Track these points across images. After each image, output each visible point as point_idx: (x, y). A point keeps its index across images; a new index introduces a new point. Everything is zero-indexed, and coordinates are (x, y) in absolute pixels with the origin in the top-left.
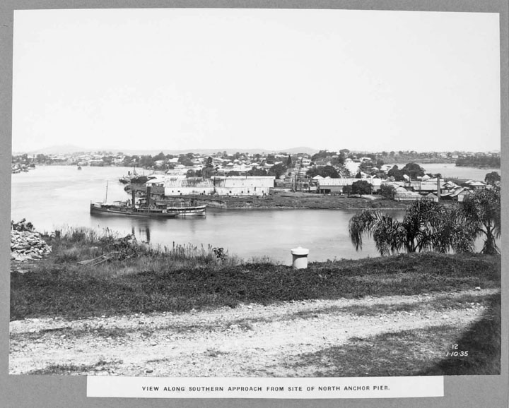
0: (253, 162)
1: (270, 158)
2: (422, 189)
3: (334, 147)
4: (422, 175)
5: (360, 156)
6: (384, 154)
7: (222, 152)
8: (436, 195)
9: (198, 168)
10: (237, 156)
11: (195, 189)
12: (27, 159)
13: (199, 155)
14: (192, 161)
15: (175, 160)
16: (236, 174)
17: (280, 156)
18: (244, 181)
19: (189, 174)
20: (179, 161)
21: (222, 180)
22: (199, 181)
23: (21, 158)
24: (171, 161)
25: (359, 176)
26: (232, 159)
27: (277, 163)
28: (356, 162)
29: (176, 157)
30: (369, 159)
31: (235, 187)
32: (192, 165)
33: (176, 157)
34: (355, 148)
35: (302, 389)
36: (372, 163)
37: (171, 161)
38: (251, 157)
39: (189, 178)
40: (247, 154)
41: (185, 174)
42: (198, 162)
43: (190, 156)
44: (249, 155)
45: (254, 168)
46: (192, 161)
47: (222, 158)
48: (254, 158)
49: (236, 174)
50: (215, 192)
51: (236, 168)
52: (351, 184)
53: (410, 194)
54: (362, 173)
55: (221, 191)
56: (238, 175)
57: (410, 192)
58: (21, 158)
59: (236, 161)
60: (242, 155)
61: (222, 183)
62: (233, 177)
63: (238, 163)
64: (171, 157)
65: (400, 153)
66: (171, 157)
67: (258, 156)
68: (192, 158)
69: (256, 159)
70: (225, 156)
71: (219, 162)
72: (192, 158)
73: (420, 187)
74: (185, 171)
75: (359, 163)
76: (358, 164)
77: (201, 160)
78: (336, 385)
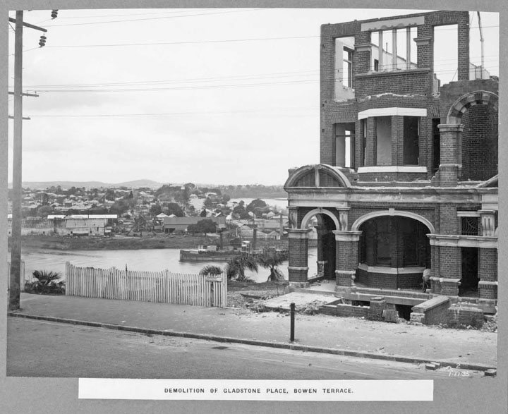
0: (91, 198)
1: (110, 193)
2: (266, 226)
3: (179, 180)
4: (268, 211)
5: (206, 190)
6: (231, 187)
7: (56, 186)
8: (278, 232)
10: (73, 191)
11: (34, 230)
17: (120, 191)
21: (63, 220)
25: (204, 214)
26: (68, 193)
27: (117, 199)
30: (215, 194)
31: (77, 225)
34: (201, 180)
35: (261, 391)
36: (216, 197)
38: (88, 192)
40: (84, 188)
44: (86, 190)
45: (94, 206)
47: (56, 193)
48: (91, 193)
50: (55, 232)
52: (196, 223)
54: (207, 210)
55: (62, 231)
59: (72, 196)
60: (78, 189)
61: (63, 224)
63: (74, 199)
65: (248, 186)
67: (96, 190)
69: (93, 194)
70: (59, 191)
71: (53, 198)
73: (263, 225)
75: (204, 199)
78: (256, 388)
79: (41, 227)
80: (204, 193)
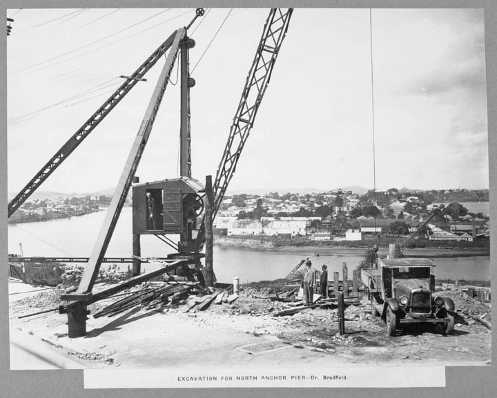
1: (320, 198)
5: (408, 195)
6: (434, 192)
8: (471, 234)
9: (249, 209)
10: (288, 196)
12: (90, 200)
13: (251, 195)
14: (245, 202)
16: (285, 215)
18: (290, 223)
19: (242, 216)
20: (233, 201)
22: (248, 223)
23: (84, 200)
25: (401, 216)
26: (284, 198)
27: (325, 203)
28: (404, 201)
29: (230, 198)
30: (416, 198)
32: (245, 205)
33: (230, 198)
38: (301, 197)
39: (240, 220)
40: (298, 194)
41: (237, 215)
43: (244, 197)
45: (302, 208)
46: (245, 202)
49: (285, 215)
51: (284, 210)
53: (446, 234)
56: (287, 216)
57: (445, 232)
58: (84, 200)
59: (287, 201)
60: (293, 195)
62: (282, 218)
63: (289, 203)
67: (308, 196)
70: (276, 196)
71: (271, 203)
73: (456, 228)
74: (237, 212)
75: (405, 203)
77: (254, 201)
79: (251, 227)
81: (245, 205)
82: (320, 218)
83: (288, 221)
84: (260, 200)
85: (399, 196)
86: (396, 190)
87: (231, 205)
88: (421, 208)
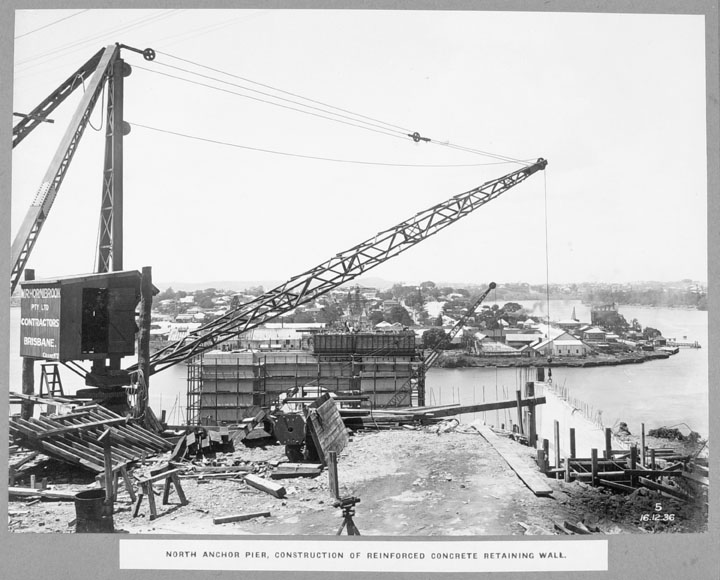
9: (221, 313)
14: (213, 300)
15: (189, 299)
20: (195, 300)
24: (182, 300)
25: (440, 321)
28: (439, 301)
29: (191, 294)
30: (460, 295)
33: (191, 294)
34: (441, 280)
37: (182, 300)
42: (222, 302)
43: (211, 293)
46: (213, 300)
64: (183, 295)
66: (183, 295)
68: (213, 296)
72: (213, 296)
76: (443, 304)
80: (446, 295)
81: (212, 305)
82: (324, 325)
83: (276, 329)
84: (236, 297)
85: (436, 295)
86: (433, 285)
87: (192, 305)
88: (466, 310)
